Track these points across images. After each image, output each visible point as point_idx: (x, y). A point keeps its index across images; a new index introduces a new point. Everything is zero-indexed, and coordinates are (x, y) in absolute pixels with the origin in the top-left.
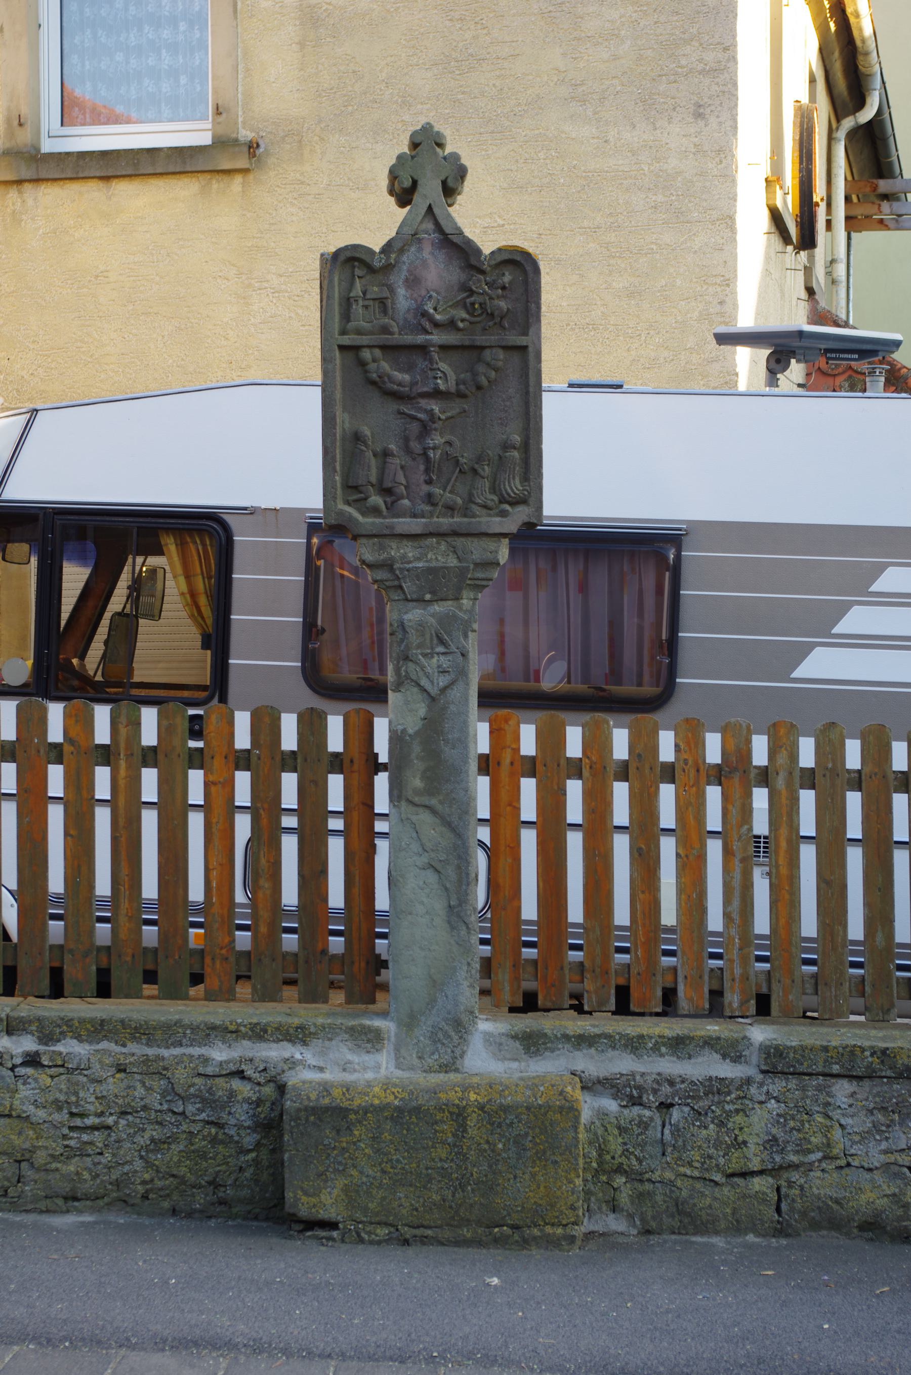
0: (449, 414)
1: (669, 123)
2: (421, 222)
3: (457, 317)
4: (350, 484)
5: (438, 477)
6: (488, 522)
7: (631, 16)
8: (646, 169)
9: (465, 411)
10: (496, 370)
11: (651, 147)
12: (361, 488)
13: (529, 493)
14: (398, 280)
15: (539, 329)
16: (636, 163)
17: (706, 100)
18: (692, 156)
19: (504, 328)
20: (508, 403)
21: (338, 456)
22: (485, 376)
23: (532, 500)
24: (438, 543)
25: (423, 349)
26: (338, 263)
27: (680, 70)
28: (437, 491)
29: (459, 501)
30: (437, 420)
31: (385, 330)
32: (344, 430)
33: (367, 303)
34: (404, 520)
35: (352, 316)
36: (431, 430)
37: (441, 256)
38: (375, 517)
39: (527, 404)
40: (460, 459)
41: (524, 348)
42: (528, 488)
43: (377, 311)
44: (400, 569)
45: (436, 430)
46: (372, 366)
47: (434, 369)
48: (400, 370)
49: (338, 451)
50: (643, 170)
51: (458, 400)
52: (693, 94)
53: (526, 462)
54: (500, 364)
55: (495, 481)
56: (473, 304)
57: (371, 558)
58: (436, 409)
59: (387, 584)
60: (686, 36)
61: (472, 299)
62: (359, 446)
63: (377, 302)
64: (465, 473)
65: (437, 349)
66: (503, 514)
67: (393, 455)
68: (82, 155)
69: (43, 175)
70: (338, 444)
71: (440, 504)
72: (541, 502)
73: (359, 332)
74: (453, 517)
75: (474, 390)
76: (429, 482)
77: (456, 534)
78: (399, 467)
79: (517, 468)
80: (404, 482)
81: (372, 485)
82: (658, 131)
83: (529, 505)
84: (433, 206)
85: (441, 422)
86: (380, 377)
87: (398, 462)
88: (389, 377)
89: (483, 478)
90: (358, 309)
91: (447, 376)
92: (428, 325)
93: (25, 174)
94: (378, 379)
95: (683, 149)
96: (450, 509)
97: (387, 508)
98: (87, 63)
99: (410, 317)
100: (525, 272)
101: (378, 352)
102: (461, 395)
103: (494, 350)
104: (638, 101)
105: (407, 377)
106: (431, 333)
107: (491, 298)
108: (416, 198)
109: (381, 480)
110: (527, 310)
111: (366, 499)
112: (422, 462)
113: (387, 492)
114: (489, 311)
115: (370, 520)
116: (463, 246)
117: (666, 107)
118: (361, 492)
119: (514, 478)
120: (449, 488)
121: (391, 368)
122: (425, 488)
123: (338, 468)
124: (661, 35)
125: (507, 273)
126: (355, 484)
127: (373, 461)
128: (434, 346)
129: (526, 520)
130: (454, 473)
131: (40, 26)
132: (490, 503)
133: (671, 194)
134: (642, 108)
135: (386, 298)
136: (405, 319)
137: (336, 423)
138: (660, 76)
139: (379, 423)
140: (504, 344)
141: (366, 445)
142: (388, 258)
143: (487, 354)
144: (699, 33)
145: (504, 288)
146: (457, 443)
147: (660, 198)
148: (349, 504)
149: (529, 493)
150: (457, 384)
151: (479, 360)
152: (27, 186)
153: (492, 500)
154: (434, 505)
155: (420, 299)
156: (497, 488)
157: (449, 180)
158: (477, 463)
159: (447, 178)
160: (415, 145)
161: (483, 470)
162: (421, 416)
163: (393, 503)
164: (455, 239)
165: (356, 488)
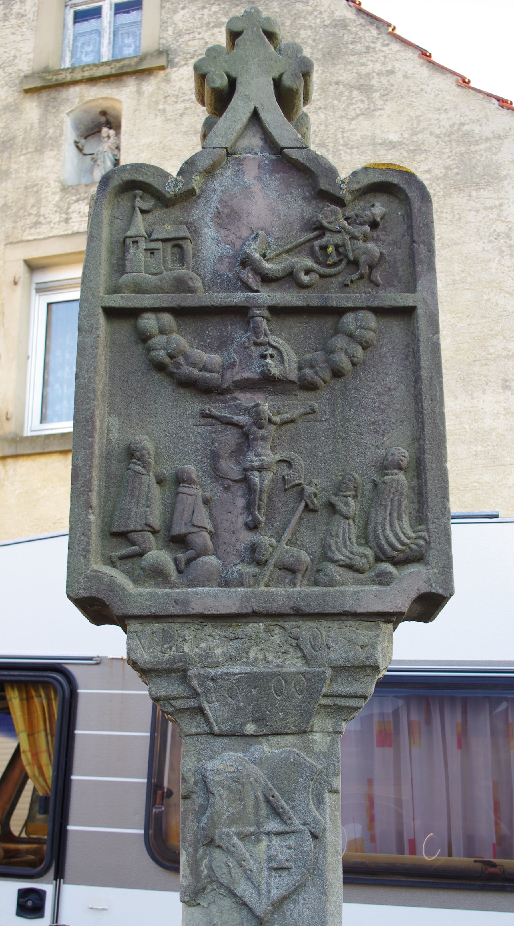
0: (287, 416)
1: (484, 394)
2: (241, 135)
3: (298, 266)
4: (115, 529)
5: (268, 519)
6: (355, 593)
7: (450, 321)
8: (467, 428)
9: (314, 411)
10: (365, 346)
11: (470, 412)
12: (133, 535)
13: (428, 543)
14: (203, 214)
15: (434, 282)
16: (459, 424)
17: (511, 376)
18: (502, 417)
19: (377, 285)
20: (386, 399)
21: (95, 482)
22: (346, 353)
23: (432, 555)
24: (268, 631)
25: (241, 313)
26: (110, 189)
27: (489, 356)
28: (265, 539)
29: (305, 557)
30: (266, 422)
31: (181, 285)
32: (109, 442)
33: (152, 245)
34: (205, 589)
35: (128, 264)
36: (256, 439)
37: (275, 182)
38: (157, 585)
39: (418, 398)
40: (306, 487)
41: (407, 313)
42: (425, 534)
43: (169, 258)
44: (199, 676)
45: (264, 439)
46: (159, 340)
47: (261, 344)
48: (205, 348)
49: (95, 473)
50: (465, 428)
51: (301, 395)
52: (500, 372)
53: (420, 493)
54: (370, 335)
55: (367, 524)
56: (324, 248)
57: (147, 657)
58: (265, 407)
59: (178, 704)
60: (493, 333)
61: (323, 241)
62: (132, 466)
63: (169, 245)
64: (314, 511)
65: (266, 313)
66: (383, 579)
67: (190, 481)
68: (48, 437)
69: (20, 451)
70: (96, 462)
71: (272, 562)
72: (449, 558)
73: (138, 289)
74: (294, 585)
75: (328, 376)
76: (253, 527)
77: (300, 614)
78: (200, 502)
79: (405, 502)
80: (210, 527)
81: (154, 532)
82: (475, 400)
83: (428, 564)
84: (260, 111)
85: (273, 428)
86: (171, 356)
87: (200, 492)
88: (186, 357)
89: (348, 518)
90: (137, 255)
91: (286, 352)
92: (251, 279)
93: (8, 451)
94: (167, 360)
95: (496, 412)
96: (290, 570)
97: (180, 572)
98: (65, 388)
99: (223, 268)
100: (406, 201)
101: (167, 319)
102: (309, 387)
103: (361, 314)
104: (459, 380)
105: (216, 359)
106: (257, 291)
107: (354, 238)
108: (236, 101)
109: (169, 525)
110: (412, 255)
111: (141, 555)
112: (240, 493)
113: (179, 542)
114: (351, 256)
115: (146, 590)
116: (308, 164)
117: (480, 383)
118: (133, 543)
119: (400, 518)
120: (287, 536)
121: (191, 345)
122: (247, 537)
123: (95, 501)
124: (474, 333)
125: (378, 204)
126: (123, 529)
127: (156, 491)
128: (260, 307)
129: (425, 589)
130: (294, 510)
131: (28, 357)
132: (358, 561)
133: (488, 445)
134: (462, 384)
135: (184, 238)
136: (216, 272)
137: (94, 428)
138: (474, 361)
139: (172, 431)
140: (375, 304)
141: (144, 464)
142: (189, 180)
143: (349, 320)
144: (503, 330)
145: (374, 225)
146: (301, 462)
147: (479, 448)
148: (113, 564)
149: (428, 543)
150: (300, 368)
151: (336, 332)
152: (10, 461)
153: (364, 555)
154: (261, 564)
155: (239, 243)
156: (371, 536)
157: (284, 78)
158: (336, 495)
159: (281, 75)
160: (234, 36)
161: (347, 504)
162: (241, 419)
163: (189, 561)
164: (294, 154)
165: (123, 536)
